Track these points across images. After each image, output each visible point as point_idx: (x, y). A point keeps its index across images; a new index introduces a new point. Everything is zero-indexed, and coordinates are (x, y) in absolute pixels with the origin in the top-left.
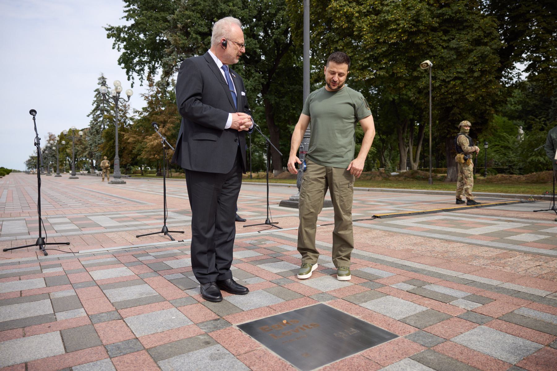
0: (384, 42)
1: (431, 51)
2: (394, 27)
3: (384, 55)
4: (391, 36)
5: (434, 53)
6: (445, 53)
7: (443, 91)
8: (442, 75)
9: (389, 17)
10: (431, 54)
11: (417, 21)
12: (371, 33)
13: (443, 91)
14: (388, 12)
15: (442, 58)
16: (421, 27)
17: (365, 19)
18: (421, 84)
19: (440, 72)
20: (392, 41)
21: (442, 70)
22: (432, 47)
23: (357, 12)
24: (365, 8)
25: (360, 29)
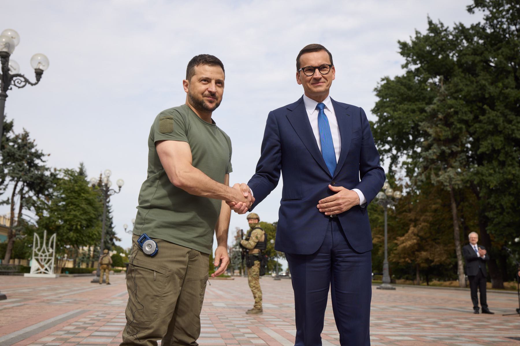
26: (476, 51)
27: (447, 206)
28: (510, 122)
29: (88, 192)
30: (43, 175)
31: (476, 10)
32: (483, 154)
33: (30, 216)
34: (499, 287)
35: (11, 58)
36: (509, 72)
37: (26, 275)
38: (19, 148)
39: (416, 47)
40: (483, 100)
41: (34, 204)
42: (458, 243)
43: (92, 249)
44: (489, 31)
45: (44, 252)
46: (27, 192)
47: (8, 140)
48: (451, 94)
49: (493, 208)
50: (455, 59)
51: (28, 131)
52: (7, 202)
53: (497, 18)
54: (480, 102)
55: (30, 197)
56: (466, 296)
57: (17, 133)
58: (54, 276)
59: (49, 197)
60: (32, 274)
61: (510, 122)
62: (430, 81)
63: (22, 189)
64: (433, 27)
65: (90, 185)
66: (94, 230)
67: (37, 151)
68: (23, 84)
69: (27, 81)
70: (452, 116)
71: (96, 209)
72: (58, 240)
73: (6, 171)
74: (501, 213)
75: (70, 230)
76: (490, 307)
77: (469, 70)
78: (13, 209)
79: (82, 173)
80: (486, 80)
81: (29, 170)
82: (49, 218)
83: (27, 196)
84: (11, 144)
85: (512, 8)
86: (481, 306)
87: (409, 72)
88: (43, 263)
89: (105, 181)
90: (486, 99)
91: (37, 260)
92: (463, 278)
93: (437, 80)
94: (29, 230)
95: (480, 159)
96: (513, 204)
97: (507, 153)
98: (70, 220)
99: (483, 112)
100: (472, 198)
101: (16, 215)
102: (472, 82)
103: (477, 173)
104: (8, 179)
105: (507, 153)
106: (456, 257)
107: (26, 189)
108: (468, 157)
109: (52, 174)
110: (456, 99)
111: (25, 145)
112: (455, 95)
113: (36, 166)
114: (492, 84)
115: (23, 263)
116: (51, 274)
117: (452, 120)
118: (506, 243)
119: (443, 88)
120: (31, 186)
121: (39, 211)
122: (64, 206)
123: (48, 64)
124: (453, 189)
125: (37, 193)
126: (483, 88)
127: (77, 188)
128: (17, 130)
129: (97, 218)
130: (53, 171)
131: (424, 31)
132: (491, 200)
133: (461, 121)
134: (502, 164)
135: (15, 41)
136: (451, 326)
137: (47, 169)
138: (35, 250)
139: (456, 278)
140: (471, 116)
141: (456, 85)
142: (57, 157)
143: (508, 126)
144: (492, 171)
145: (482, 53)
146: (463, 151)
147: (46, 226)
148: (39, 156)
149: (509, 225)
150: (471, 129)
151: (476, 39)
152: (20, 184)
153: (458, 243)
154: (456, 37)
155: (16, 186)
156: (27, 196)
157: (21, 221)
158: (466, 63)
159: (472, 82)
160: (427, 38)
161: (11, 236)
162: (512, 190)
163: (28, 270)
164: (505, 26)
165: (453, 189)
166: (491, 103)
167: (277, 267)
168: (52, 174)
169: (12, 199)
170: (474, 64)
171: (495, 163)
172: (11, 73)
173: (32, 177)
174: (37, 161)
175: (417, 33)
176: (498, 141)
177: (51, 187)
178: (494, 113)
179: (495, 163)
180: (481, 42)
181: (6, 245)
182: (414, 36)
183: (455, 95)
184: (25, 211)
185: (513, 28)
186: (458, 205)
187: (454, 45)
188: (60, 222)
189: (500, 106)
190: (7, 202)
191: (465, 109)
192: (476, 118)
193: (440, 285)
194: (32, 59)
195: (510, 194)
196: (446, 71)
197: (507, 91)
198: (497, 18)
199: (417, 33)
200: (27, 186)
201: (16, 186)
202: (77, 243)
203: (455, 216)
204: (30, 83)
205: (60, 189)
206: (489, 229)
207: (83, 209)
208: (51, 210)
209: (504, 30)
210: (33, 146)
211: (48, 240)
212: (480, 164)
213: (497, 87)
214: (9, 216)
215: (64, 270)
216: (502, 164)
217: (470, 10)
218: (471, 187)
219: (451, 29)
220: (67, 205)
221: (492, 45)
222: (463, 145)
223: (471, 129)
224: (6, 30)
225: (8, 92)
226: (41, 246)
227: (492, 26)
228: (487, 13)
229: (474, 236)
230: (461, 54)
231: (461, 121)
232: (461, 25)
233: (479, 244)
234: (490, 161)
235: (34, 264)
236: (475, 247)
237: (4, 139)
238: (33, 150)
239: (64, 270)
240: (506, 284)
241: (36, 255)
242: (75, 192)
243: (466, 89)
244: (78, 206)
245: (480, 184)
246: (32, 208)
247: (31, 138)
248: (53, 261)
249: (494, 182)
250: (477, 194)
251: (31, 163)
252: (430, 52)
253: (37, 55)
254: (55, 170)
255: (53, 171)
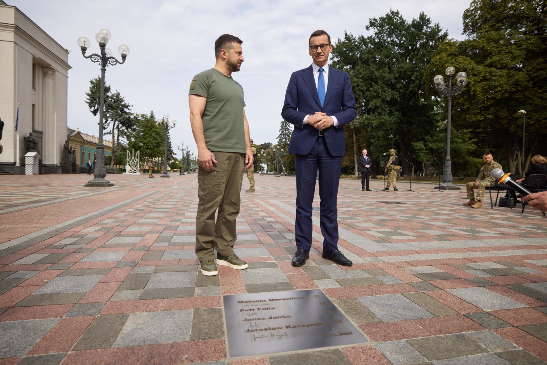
0: (492, 98)
1: (527, 101)
2: (499, 89)
3: (492, 105)
4: (497, 94)
5: (531, 102)
6: (538, 101)
7: (536, 126)
8: (535, 116)
9: (497, 83)
10: (528, 102)
11: (517, 85)
12: (482, 92)
13: (536, 126)
14: (495, 81)
15: (536, 105)
16: (519, 88)
17: (479, 84)
18: (519, 123)
19: (534, 114)
20: (498, 98)
21: (536, 112)
22: (529, 98)
23: (473, 81)
24: (479, 78)
25: (475, 91)
26: (369, 52)
27: (351, 136)
28: (385, 91)
29: (156, 128)
30: (130, 118)
31: (370, 28)
32: (370, 108)
33: (124, 141)
34: (374, 178)
35: (106, 47)
36: (386, 64)
37: (124, 173)
38: (115, 102)
39: (338, 48)
40: (372, 79)
41: (125, 134)
42: (355, 156)
43: (160, 159)
44: (377, 41)
45: (133, 161)
46: (121, 127)
47: (108, 97)
48: (355, 76)
49: (374, 137)
50: (358, 56)
51: (119, 92)
52: (110, 133)
53: (381, 34)
54: (371, 80)
55: (123, 130)
56: (359, 183)
57: (113, 93)
58: (140, 174)
59: (134, 130)
60: (127, 173)
61: (385, 91)
62: (345, 67)
63: (118, 126)
64: (347, 37)
65: (157, 124)
66: (161, 149)
67: (125, 104)
68: (115, 63)
69: (117, 61)
70: (355, 88)
71: (161, 137)
72: (141, 154)
73: (108, 115)
74: (378, 140)
75: (147, 149)
76: (370, 188)
77: (366, 62)
78: (113, 137)
79: (152, 117)
80: (374, 68)
81: (122, 114)
82: (135, 142)
83: (121, 129)
84: (110, 99)
85: (389, 28)
86: (366, 187)
87: (334, 62)
88: (133, 167)
89: (165, 121)
90: (373, 79)
91: (130, 165)
92: (357, 173)
93: (348, 67)
94: (124, 149)
95: (368, 111)
96: (384, 135)
97: (382, 108)
98: (147, 143)
99: (372, 86)
100: (364, 132)
101: (116, 140)
102: (367, 69)
103: (367, 119)
104: (109, 120)
105: (382, 108)
106: (354, 163)
107: (121, 125)
108: (363, 110)
109: (135, 117)
110: (358, 78)
111: (118, 100)
112: (358, 76)
113: (125, 112)
114: (377, 70)
115: (122, 167)
116: (138, 173)
117: (355, 90)
118: (379, 155)
119: (351, 72)
120: (123, 124)
121: (128, 138)
122: (143, 135)
123: (129, 52)
124: (355, 127)
125: (127, 128)
126: (372, 72)
127: (149, 125)
128: (113, 91)
129: (162, 142)
130: (135, 115)
131: (343, 40)
132: (373, 133)
133: (360, 90)
134: (380, 114)
135: (108, 36)
136: (351, 197)
137: (132, 114)
138: (127, 160)
139: (354, 174)
140: (365, 88)
141: (358, 70)
142: (138, 108)
143: (384, 94)
144: (374, 118)
145: (373, 53)
146: (360, 107)
147: (134, 147)
148: (127, 107)
149: (381, 146)
150: (365, 95)
151: (369, 45)
152: (117, 123)
153: (355, 156)
154: (360, 43)
155: (114, 124)
156: (121, 129)
157: (119, 144)
158: (364, 58)
159: (367, 69)
160: (344, 43)
161: (114, 152)
162: (384, 128)
163: (125, 171)
164: (385, 38)
165: (355, 127)
166: (376, 81)
167: (262, 169)
168: (135, 117)
169: (113, 131)
170: (368, 59)
171: (376, 114)
172: (107, 56)
173: (123, 119)
174: (126, 110)
175: (339, 40)
176: (378, 102)
177: (135, 124)
178: (377, 86)
179: (376, 114)
180: (372, 46)
181: (111, 157)
182: (337, 42)
183: (358, 76)
184: (120, 138)
185: (389, 39)
186: (356, 135)
187: (358, 47)
188: (141, 144)
189: (380, 83)
190: (110, 133)
191: (362, 84)
192: (368, 89)
193: (346, 177)
194: (119, 48)
195: (383, 130)
196: (353, 62)
197: (384, 74)
198: (381, 34)
199: (339, 40)
200: (121, 123)
201: (114, 124)
202: (152, 156)
203: (354, 142)
204: (119, 62)
205: (140, 125)
206: (372, 148)
207: (154, 137)
208: (136, 138)
209: (384, 40)
210: (123, 101)
211: (135, 154)
212: (368, 114)
213: (379, 72)
214: (111, 141)
215: (145, 171)
216: (380, 114)
217: (367, 28)
218: (364, 126)
219: (357, 39)
220: (144, 135)
221: (378, 49)
222: (360, 104)
223: (365, 95)
224: (102, 30)
225: (106, 68)
226: (131, 158)
227: (378, 38)
228: (376, 30)
229: (365, 151)
230: (362, 53)
231: (360, 90)
232: (362, 37)
233: (367, 155)
234: (373, 113)
235: (128, 167)
236: (366, 157)
237: (105, 96)
238: (123, 103)
239: (145, 171)
240: (378, 176)
241: (129, 162)
242: (149, 127)
243: (363, 73)
244: (151, 135)
245: (368, 125)
246: (125, 136)
247: (121, 96)
248: (138, 165)
249: (375, 123)
250: (366, 130)
251: (122, 111)
252: (345, 51)
253: (122, 45)
254: (137, 115)
255: (135, 115)
